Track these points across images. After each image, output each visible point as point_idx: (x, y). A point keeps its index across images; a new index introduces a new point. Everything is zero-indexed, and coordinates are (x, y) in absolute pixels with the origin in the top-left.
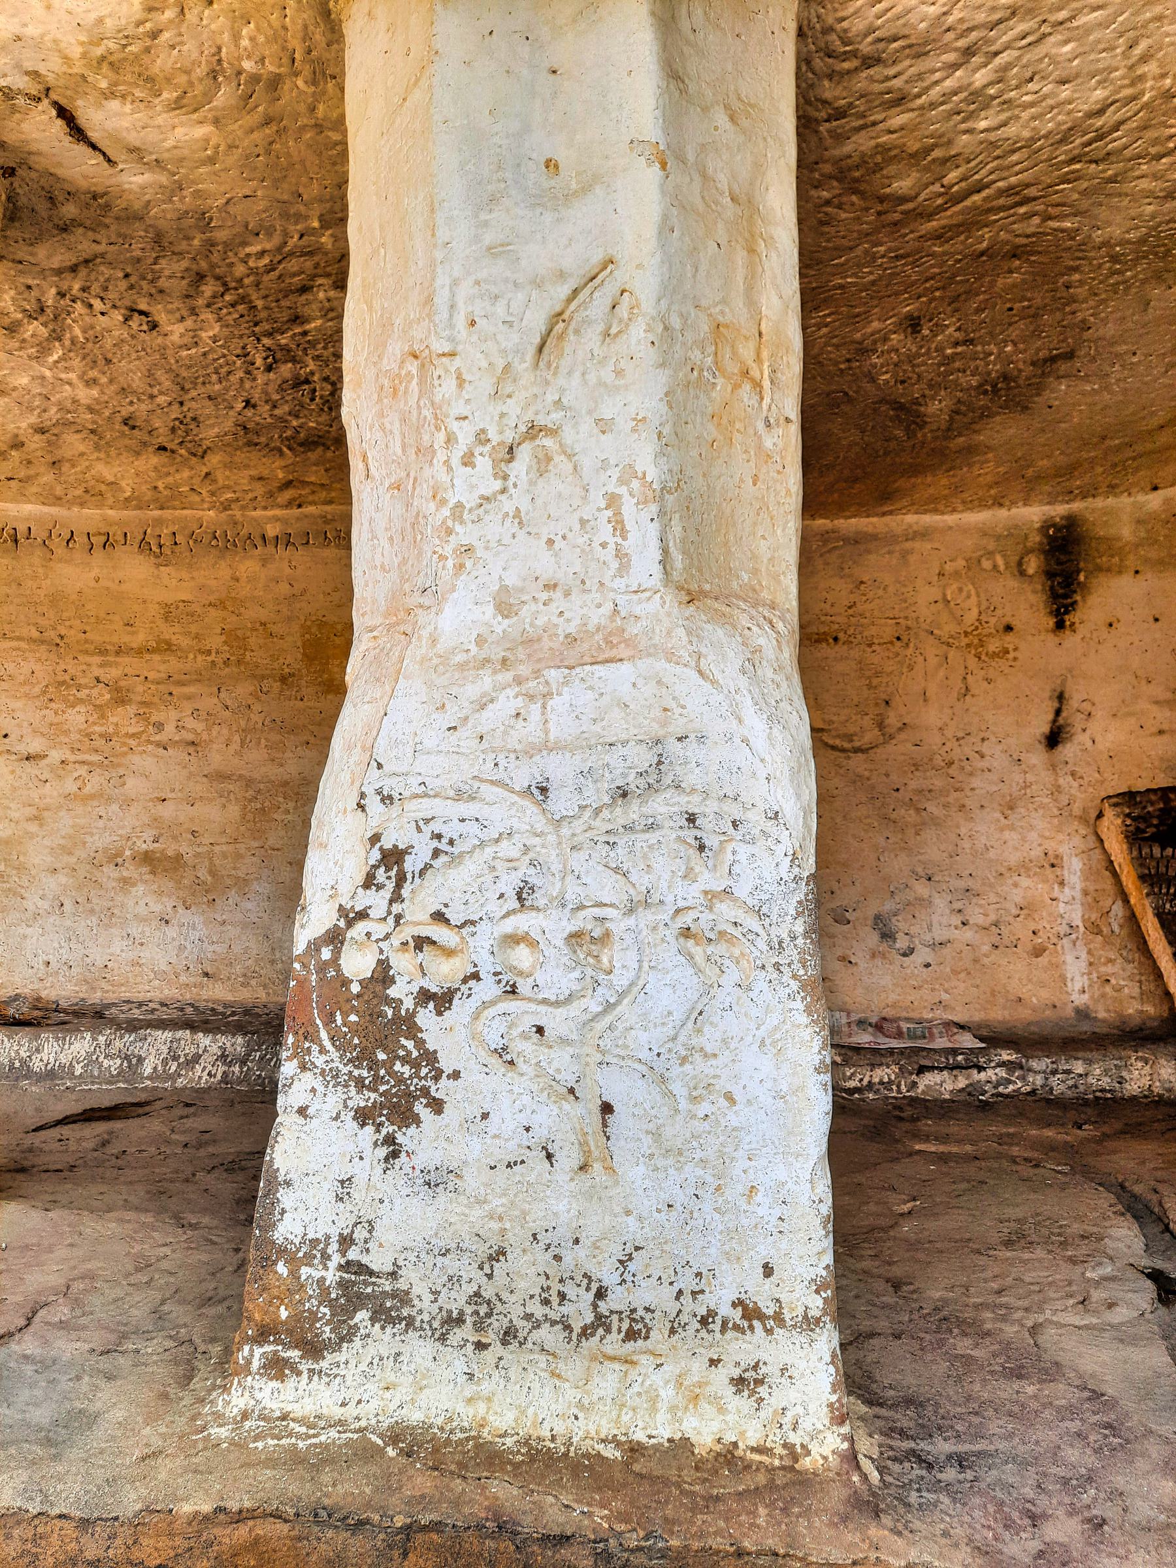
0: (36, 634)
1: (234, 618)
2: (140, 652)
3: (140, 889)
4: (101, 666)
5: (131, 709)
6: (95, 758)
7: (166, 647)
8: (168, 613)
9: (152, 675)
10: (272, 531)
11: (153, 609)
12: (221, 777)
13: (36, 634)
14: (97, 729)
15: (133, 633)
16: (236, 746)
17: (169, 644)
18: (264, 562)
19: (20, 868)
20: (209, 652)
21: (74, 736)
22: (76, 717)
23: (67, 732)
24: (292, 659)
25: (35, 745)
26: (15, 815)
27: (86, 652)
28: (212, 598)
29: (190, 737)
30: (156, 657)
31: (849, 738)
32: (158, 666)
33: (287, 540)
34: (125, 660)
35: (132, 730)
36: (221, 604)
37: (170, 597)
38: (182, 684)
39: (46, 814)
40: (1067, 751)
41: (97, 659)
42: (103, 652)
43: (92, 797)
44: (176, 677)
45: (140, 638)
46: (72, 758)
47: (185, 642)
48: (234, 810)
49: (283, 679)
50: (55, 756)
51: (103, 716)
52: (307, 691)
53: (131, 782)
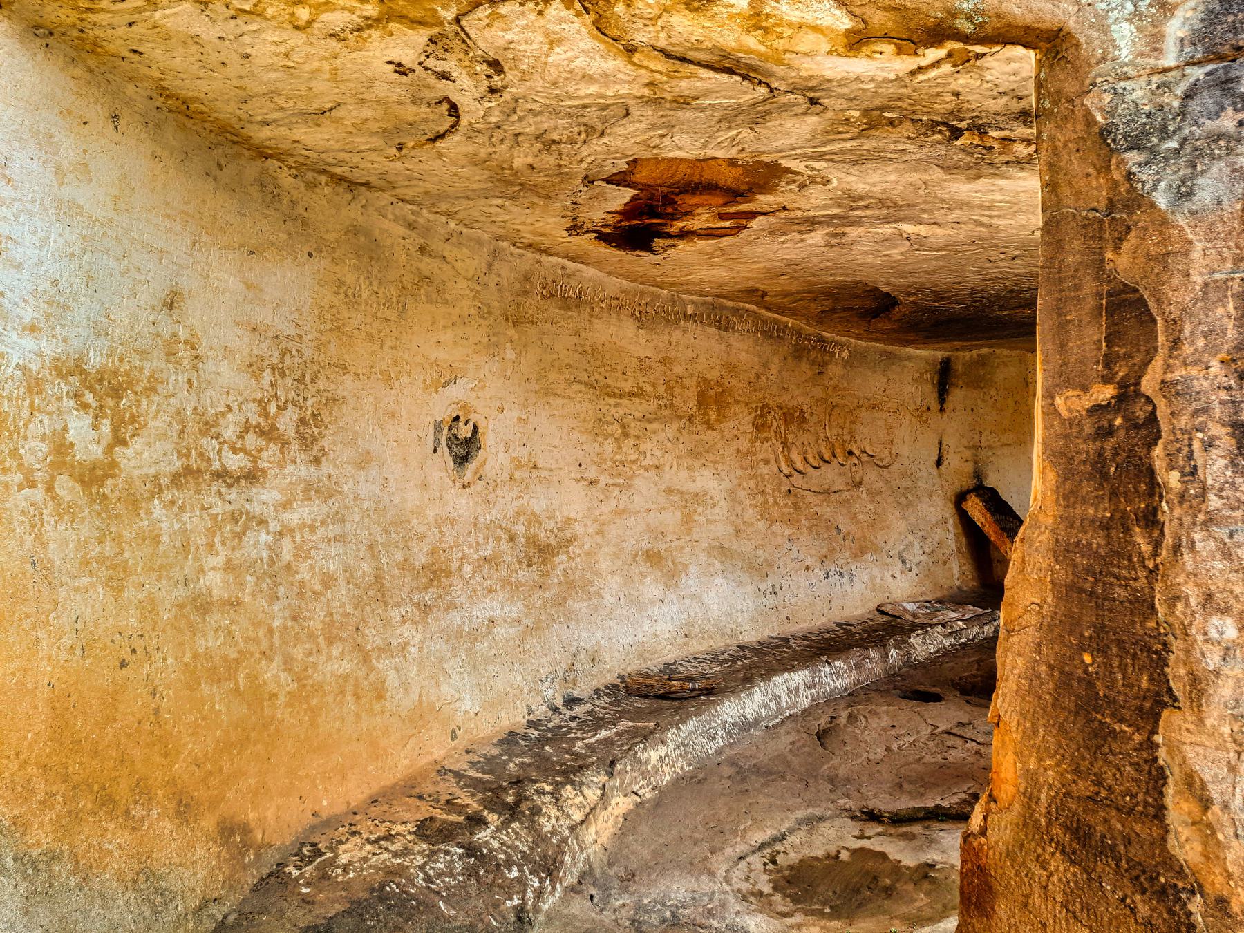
0: (586, 378)
1: (668, 373)
2: (631, 395)
3: (648, 581)
4: (615, 406)
5: (631, 441)
6: (620, 481)
7: (639, 393)
8: (644, 365)
9: (638, 415)
10: (690, 310)
11: (635, 362)
12: (670, 491)
13: (586, 378)
14: (618, 457)
15: (626, 380)
16: (675, 468)
17: (640, 388)
18: (685, 331)
19: (597, 574)
20: (658, 398)
21: (609, 464)
22: (608, 446)
23: (605, 460)
24: (693, 404)
25: (591, 473)
26: (590, 530)
27: (607, 394)
28: (660, 356)
29: (656, 462)
30: (637, 400)
31: (882, 460)
32: (638, 407)
33: (692, 318)
34: (625, 402)
35: (633, 457)
36: (662, 362)
37: (642, 355)
38: (650, 421)
39: (605, 527)
40: (943, 468)
41: (612, 401)
42: (614, 396)
43: (623, 512)
44: (648, 416)
45: (628, 386)
46: (611, 481)
47: (648, 389)
48: (678, 514)
49: (689, 419)
50: (604, 479)
51: (619, 448)
52: (700, 428)
53: (637, 498)
